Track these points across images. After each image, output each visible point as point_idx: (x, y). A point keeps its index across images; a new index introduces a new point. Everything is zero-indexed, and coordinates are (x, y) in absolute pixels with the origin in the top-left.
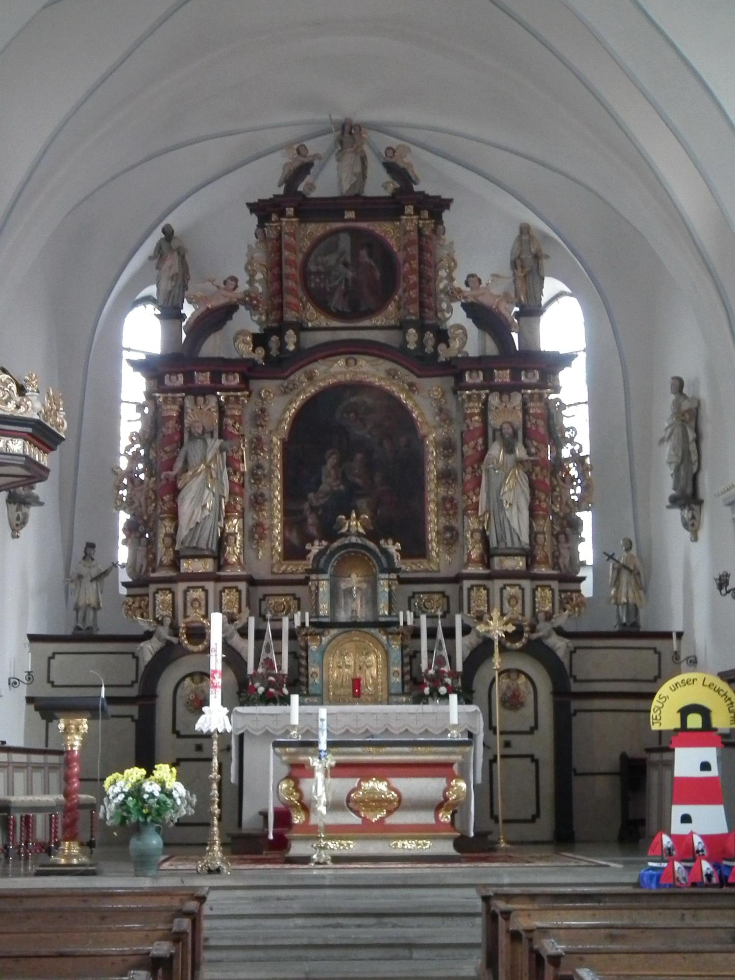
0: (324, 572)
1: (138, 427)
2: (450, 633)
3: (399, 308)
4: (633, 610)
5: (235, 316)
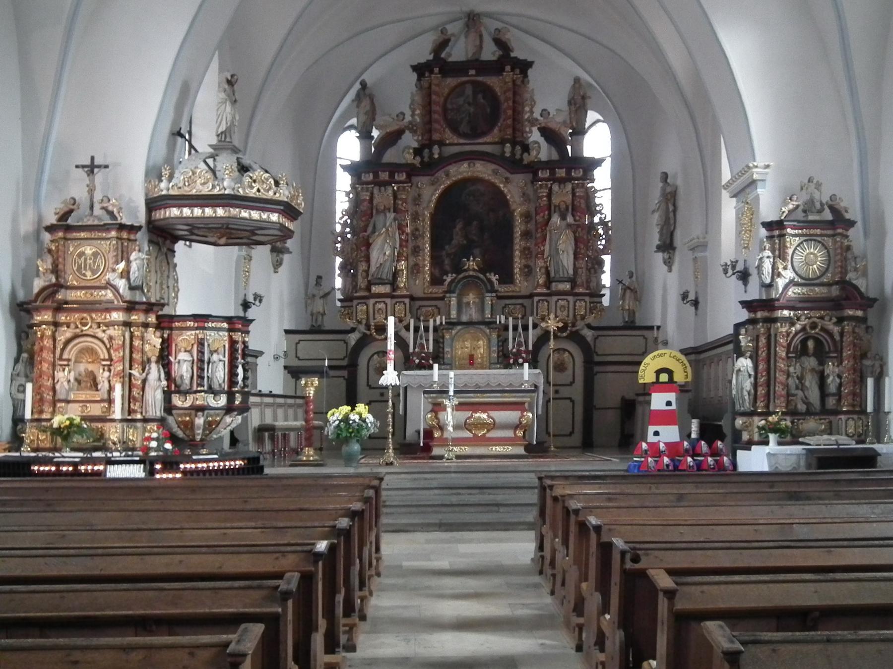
0: (454, 293)
1: (346, 206)
2: (525, 328)
3: (500, 131)
4: (632, 313)
5: (403, 137)
